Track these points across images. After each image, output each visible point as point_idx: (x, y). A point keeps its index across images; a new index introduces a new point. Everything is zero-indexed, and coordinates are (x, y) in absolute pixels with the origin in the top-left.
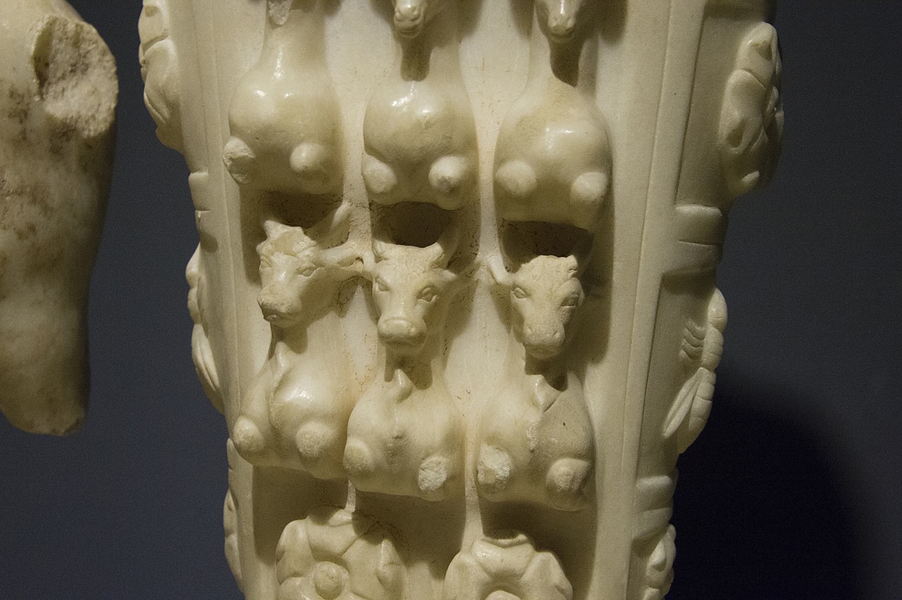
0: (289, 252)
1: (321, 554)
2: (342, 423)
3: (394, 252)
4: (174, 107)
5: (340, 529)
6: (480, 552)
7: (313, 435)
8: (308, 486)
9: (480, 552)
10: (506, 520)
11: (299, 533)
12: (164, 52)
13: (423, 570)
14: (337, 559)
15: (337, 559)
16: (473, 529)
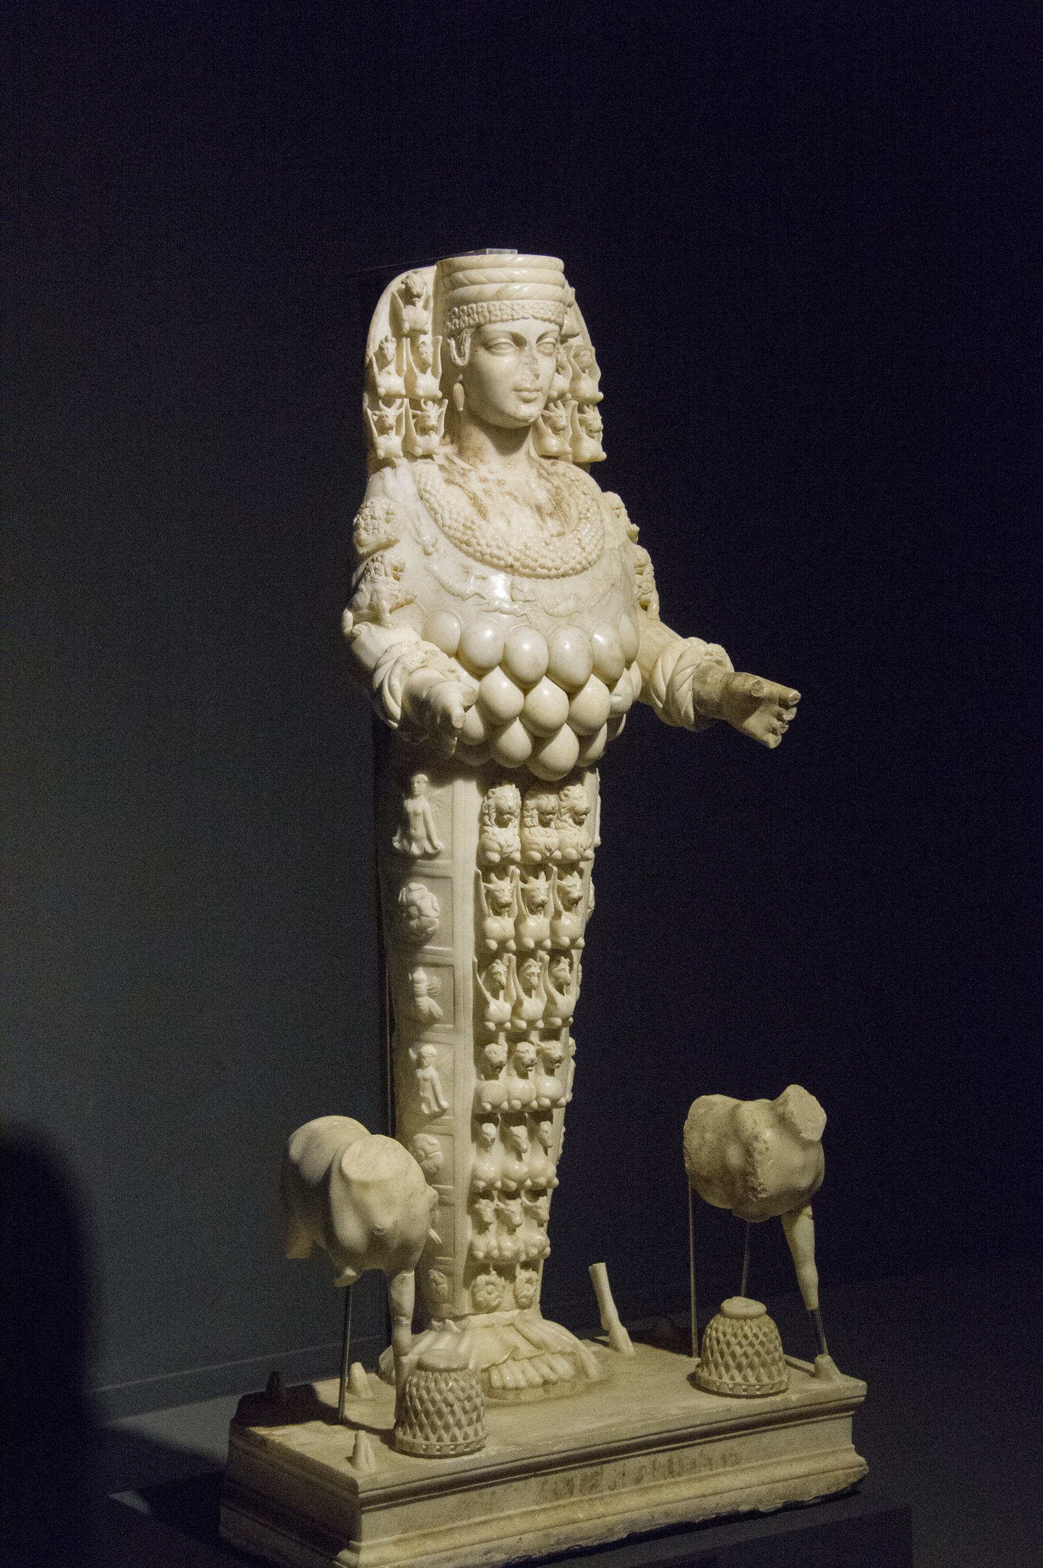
0: (487, 1208)
1: (488, 1283)
2: (500, 1249)
3: (511, 1202)
4: (438, 1168)
5: (493, 1276)
6: (522, 1275)
7: (495, 1253)
8: (477, 1267)
9: (522, 1275)
10: (526, 1266)
11: (482, 1279)
12: (438, 1156)
13: (508, 1282)
14: (493, 1284)
15: (493, 1284)
16: (518, 1269)
